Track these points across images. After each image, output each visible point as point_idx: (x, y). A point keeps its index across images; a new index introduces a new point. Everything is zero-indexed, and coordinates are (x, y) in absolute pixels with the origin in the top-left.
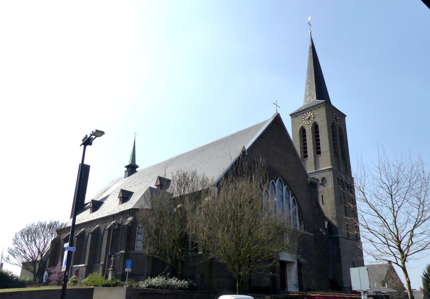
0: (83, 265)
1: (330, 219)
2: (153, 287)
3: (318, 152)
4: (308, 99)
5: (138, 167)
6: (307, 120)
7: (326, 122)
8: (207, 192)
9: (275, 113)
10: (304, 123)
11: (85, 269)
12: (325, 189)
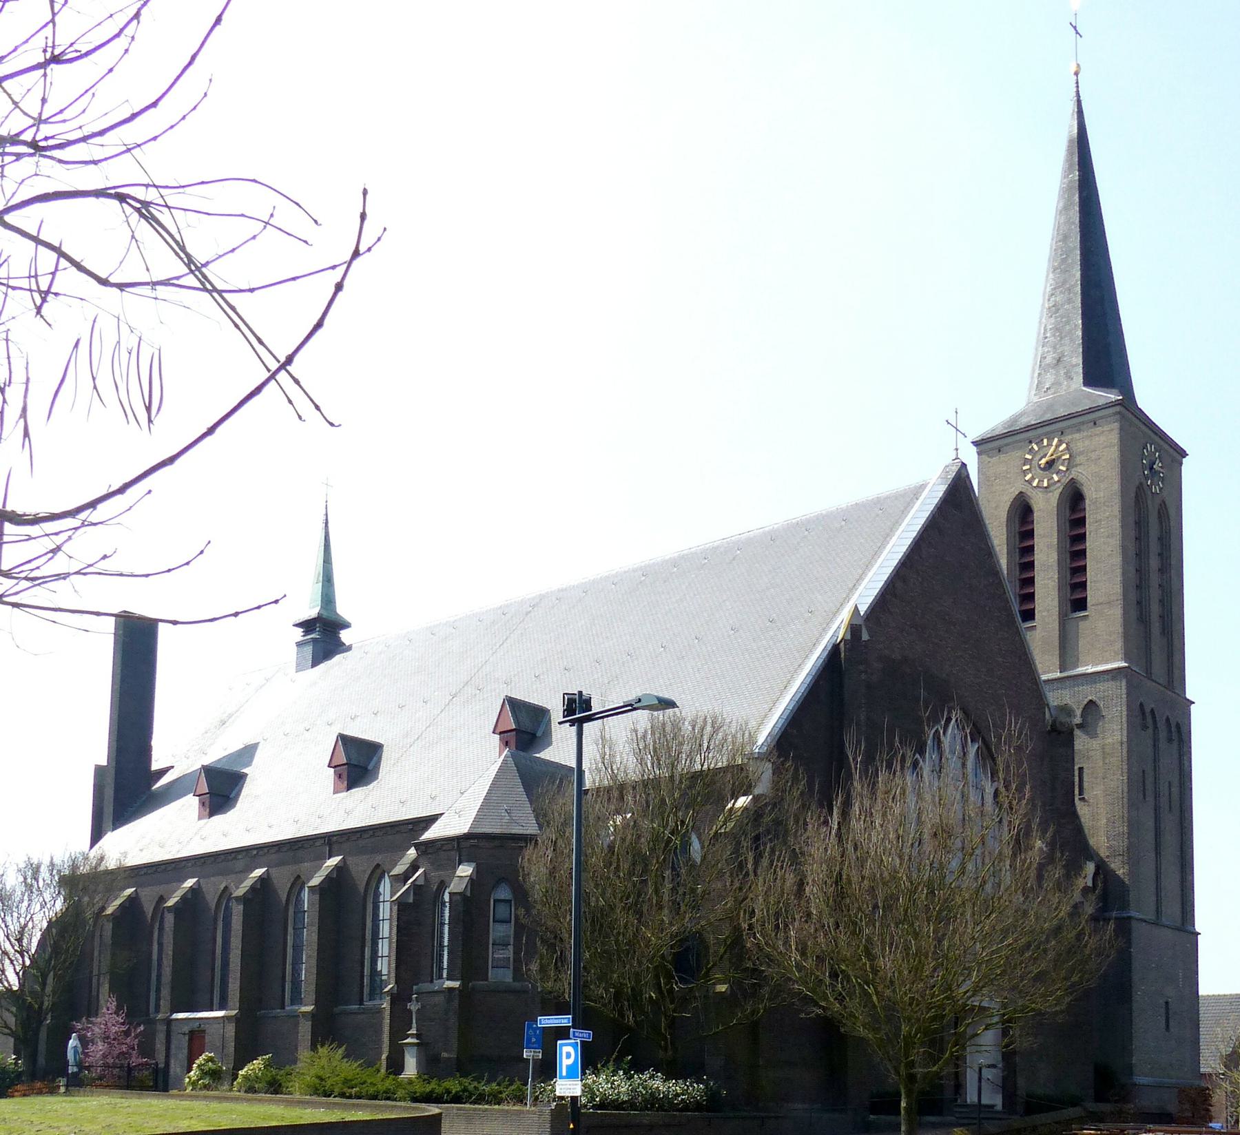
0: (221, 1014)
1: (1103, 853)
2: (617, 1105)
3: (1076, 599)
4: (1049, 379)
5: (346, 625)
6: (1044, 469)
7: (1116, 487)
8: (736, 777)
9: (949, 461)
10: (1030, 482)
11: (231, 1030)
12: (1095, 744)
